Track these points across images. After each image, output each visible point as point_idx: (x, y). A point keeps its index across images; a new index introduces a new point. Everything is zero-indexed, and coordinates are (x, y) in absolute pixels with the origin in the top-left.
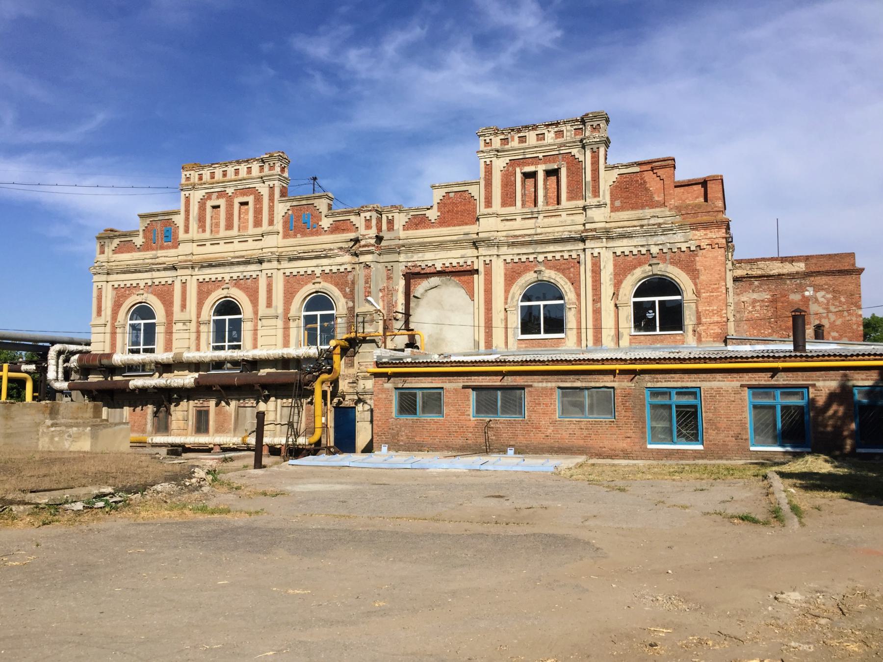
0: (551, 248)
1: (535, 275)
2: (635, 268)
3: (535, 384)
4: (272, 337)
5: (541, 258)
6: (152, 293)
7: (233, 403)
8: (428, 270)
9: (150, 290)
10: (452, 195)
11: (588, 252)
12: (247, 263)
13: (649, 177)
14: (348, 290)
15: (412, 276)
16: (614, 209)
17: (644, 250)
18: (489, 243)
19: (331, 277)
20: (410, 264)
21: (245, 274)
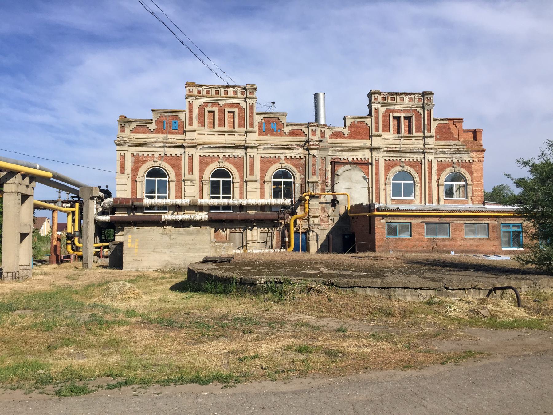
0: (408, 155)
1: (401, 168)
2: (446, 168)
3: (455, 222)
4: (253, 194)
5: (403, 160)
6: (164, 161)
7: (228, 231)
8: (344, 161)
9: (163, 159)
10: (356, 123)
11: (426, 159)
12: (236, 148)
13: (452, 126)
14: (301, 168)
15: (335, 164)
16: (436, 140)
17: (450, 160)
18: (378, 149)
19: (291, 161)
20: (334, 157)
21: (234, 154)
